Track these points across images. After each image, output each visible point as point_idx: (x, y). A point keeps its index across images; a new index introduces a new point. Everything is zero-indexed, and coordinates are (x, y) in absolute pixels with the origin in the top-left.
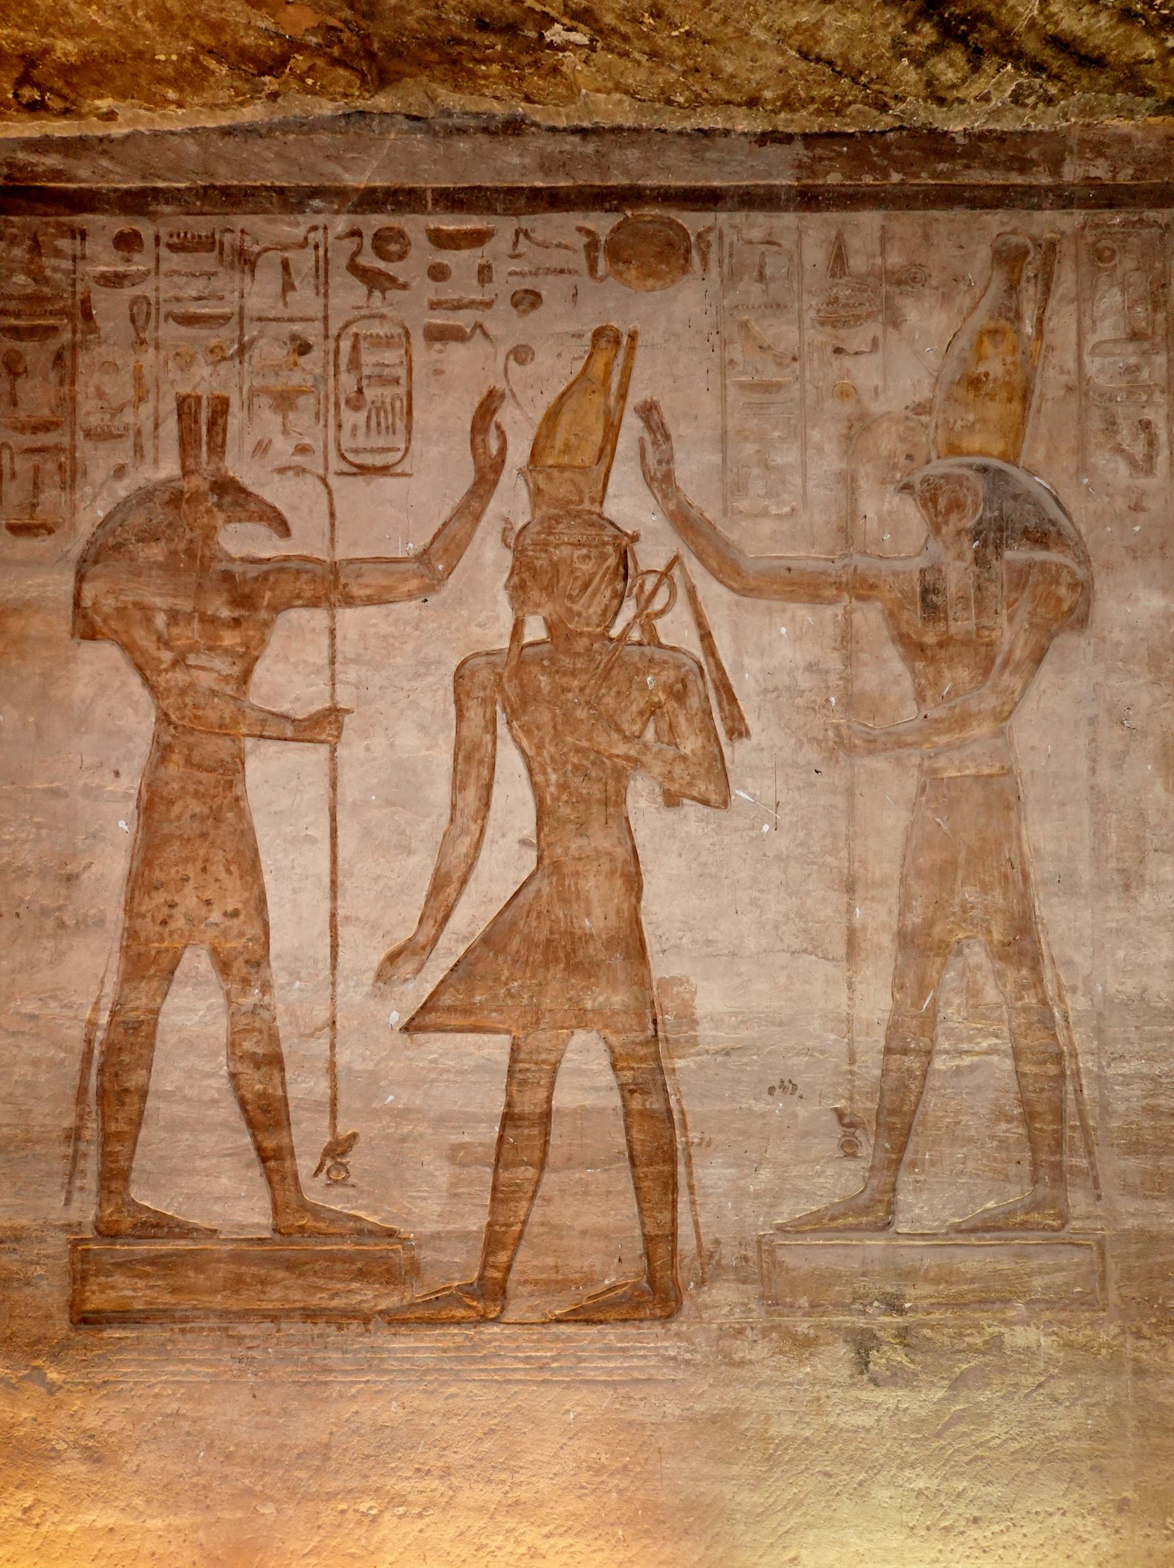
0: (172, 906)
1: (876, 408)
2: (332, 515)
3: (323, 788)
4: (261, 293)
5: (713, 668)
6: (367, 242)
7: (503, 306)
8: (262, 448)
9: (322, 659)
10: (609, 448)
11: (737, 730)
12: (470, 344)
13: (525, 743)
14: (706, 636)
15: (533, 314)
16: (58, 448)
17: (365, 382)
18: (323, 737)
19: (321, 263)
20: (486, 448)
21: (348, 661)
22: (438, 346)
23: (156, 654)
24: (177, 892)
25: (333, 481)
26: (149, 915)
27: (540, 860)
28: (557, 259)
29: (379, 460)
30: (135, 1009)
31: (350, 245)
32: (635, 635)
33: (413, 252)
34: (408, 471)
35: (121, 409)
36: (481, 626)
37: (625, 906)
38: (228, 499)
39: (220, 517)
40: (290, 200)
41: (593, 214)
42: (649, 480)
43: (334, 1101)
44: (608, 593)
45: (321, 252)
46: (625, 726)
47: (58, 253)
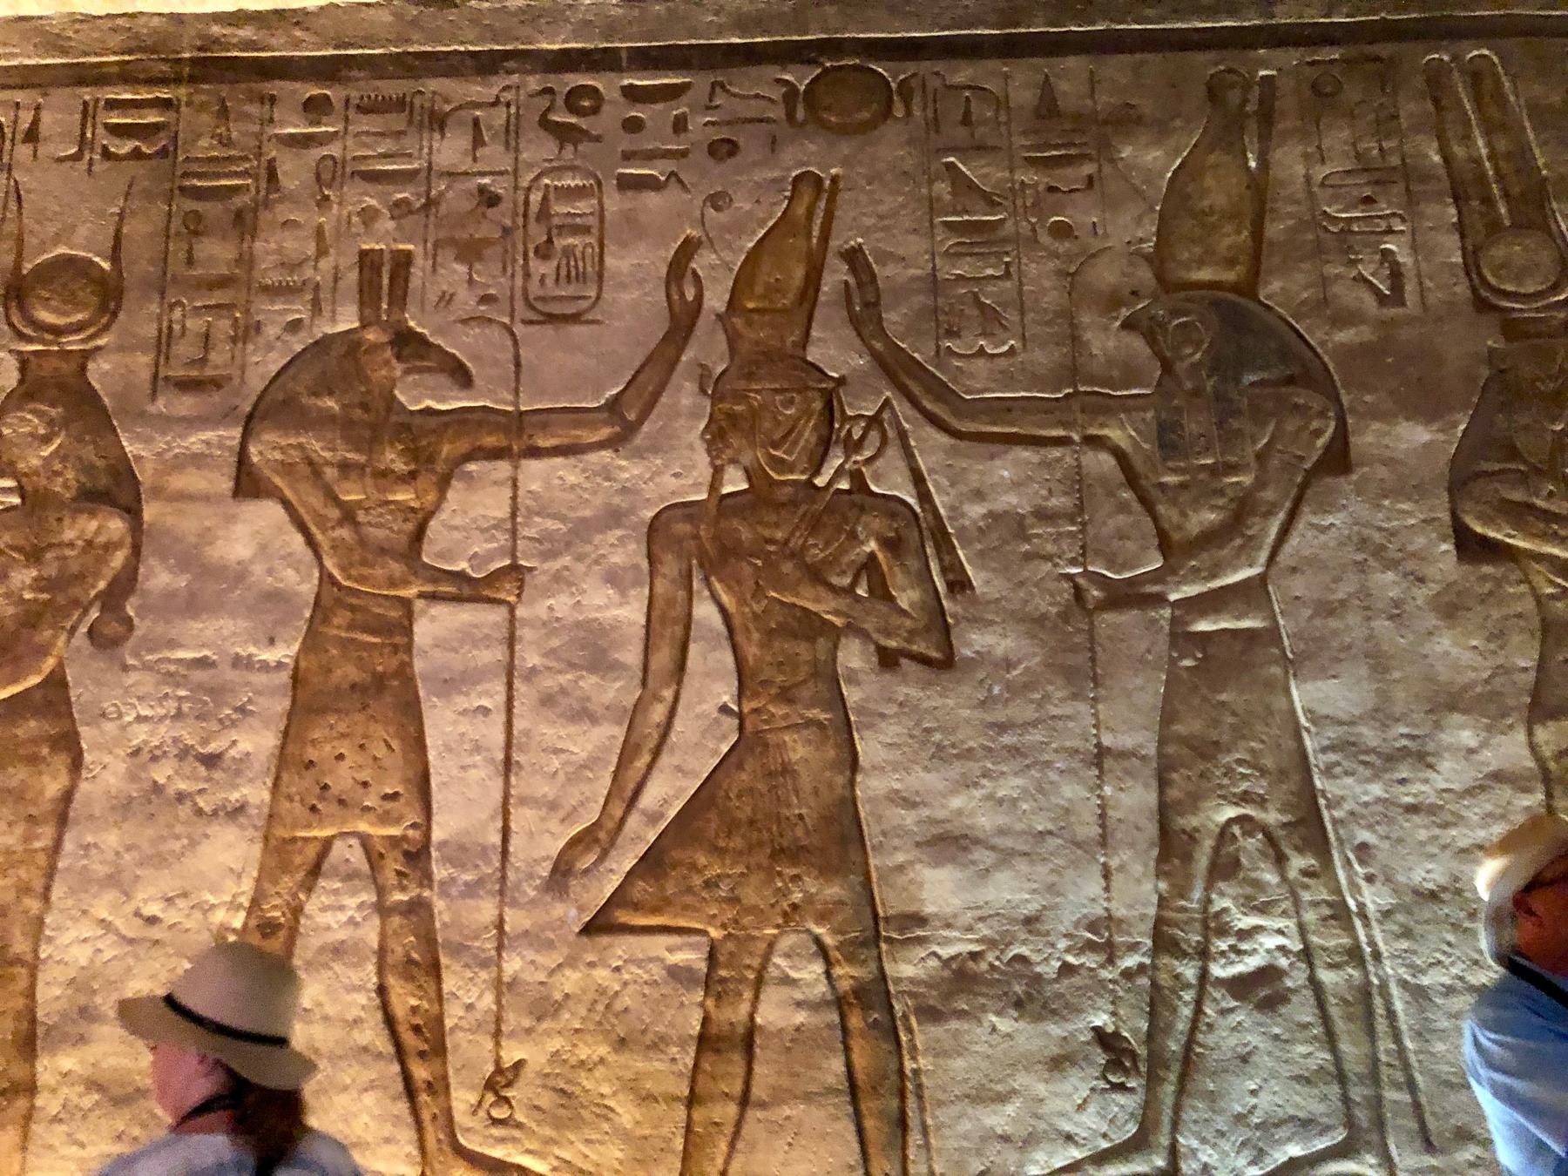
0: (325, 787)
1: (1096, 245)
2: (518, 365)
3: (498, 654)
4: (450, 150)
5: (930, 517)
6: (560, 101)
7: (700, 156)
8: (446, 299)
9: (503, 512)
10: (811, 292)
11: (960, 584)
12: (666, 192)
13: (725, 599)
14: (918, 480)
15: (731, 162)
16: (230, 307)
17: (555, 231)
18: (502, 596)
19: (513, 119)
20: (682, 295)
21: (531, 512)
22: (630, 194)
23: (323, 511)
24: (331, 772)
25: (519, 329)
26: (297, 798)
27: (741, 728)
28: (752, 109)
29: (570, 309)
30: (275, 907)
31: (544, 102)
32: (844, 485)
33: (605, 108)
34: (599, 317)
35: (300, 264)
36: (676, 475)
37: (840, 780)
38: (406, 351)
39: (399, 369)
40: (486, 65)
41: (791, 67)
42: (855, 322)
43: (499, 1020)
44: (813, 440)
45: (513, 110)
46: (835, 580)
47: (247, 116)
